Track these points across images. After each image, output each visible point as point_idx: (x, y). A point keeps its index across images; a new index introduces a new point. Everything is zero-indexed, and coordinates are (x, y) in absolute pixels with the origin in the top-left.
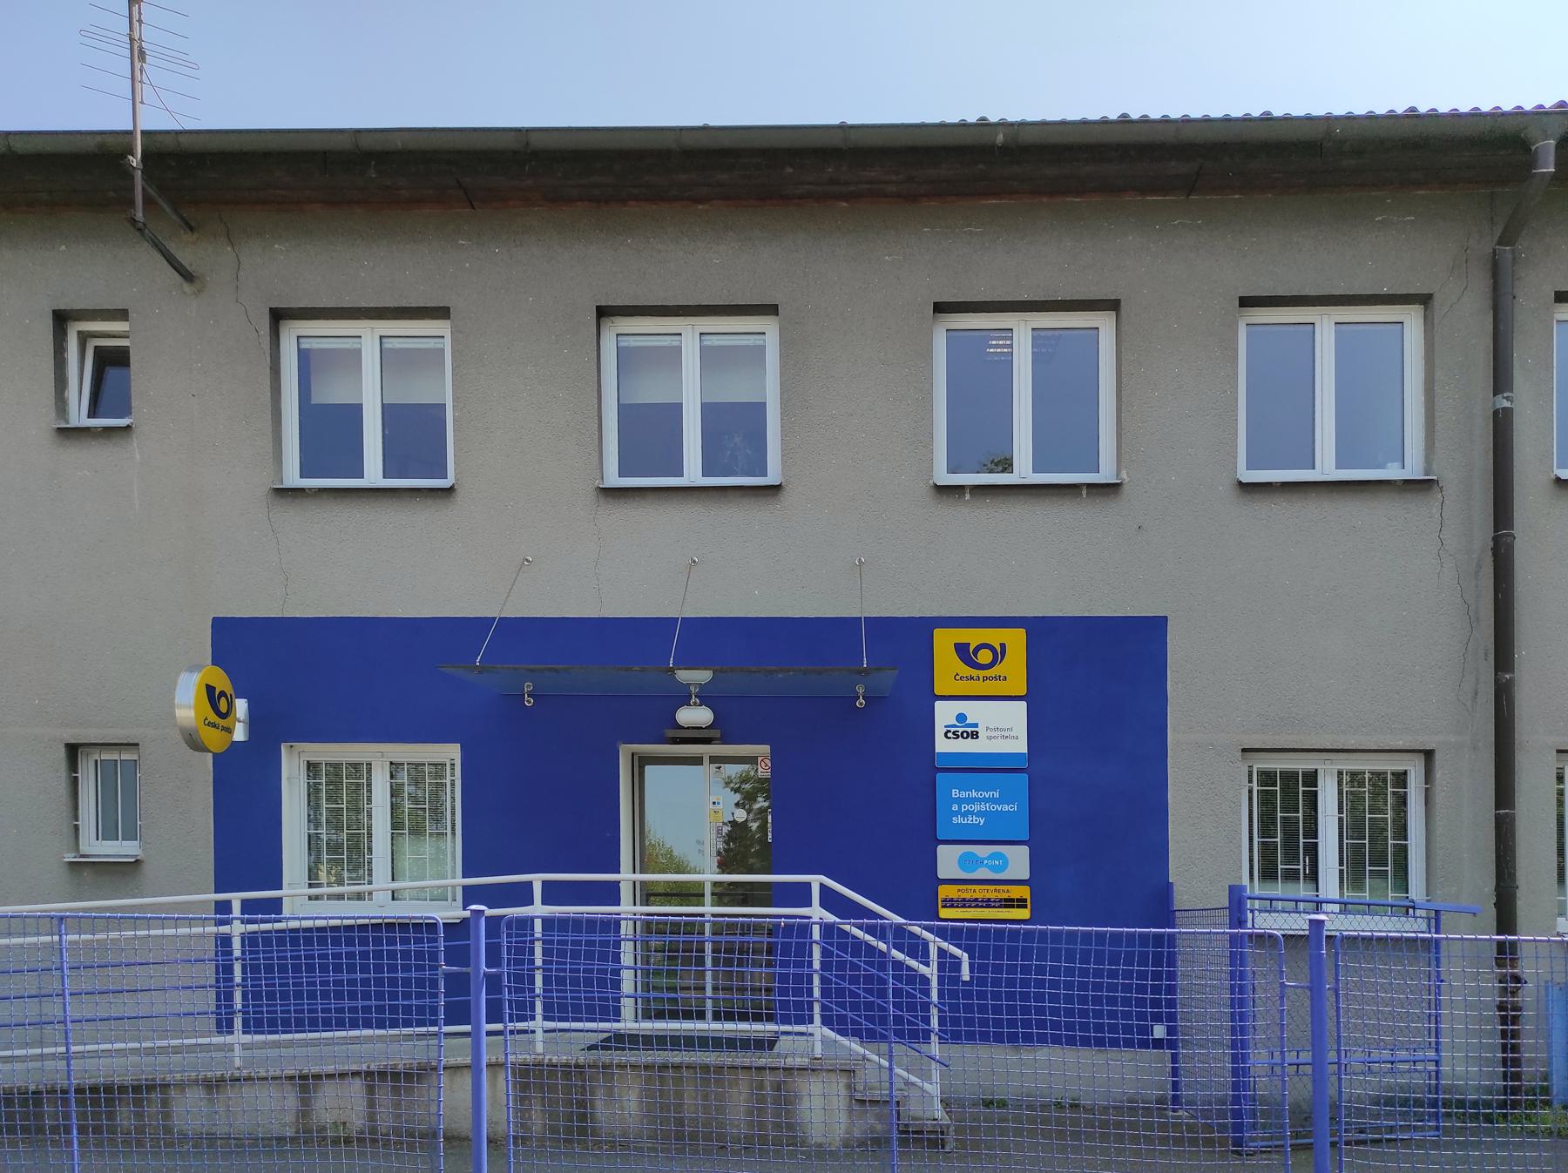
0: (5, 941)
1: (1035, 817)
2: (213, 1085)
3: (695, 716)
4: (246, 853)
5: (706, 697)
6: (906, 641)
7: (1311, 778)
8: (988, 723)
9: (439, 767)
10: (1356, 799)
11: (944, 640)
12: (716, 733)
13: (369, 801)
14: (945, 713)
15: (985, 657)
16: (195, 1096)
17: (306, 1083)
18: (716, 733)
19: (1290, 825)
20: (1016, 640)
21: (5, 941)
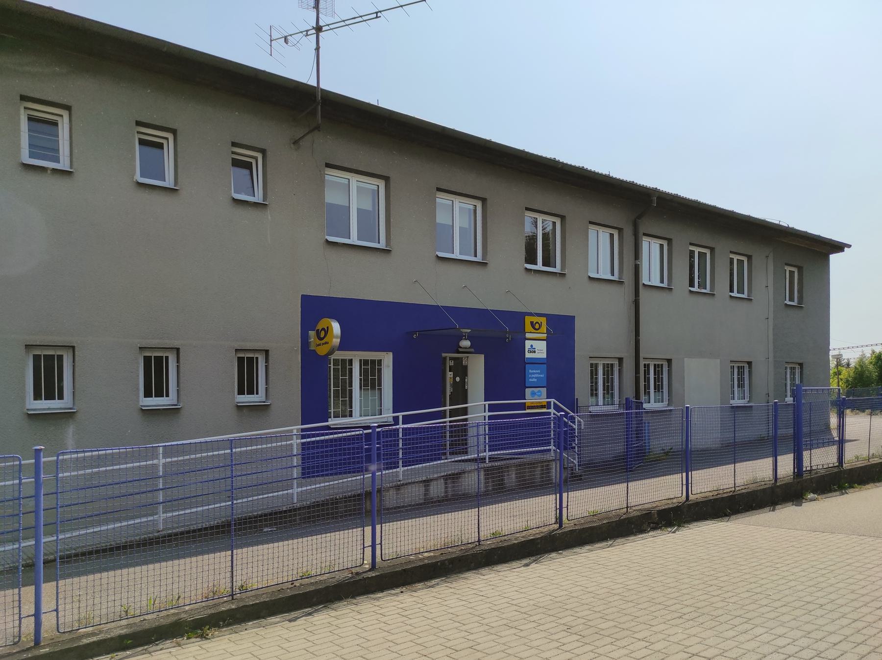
0: (3, 484)
1: (548, 378)
2: (398, 487)
3: (466, 343)
4: (314, 407)
5: (469, 338)
6: (516, 320)
7: (351, 361)
8: (537, 348)
9: (612, 365)
10: (366, 371)
11: (528, 320)
12: (472, 350)
13: (361, 380)
14: (528, 344)
15: (537, 326)
16: (392, 492)
17: (427, 482)
18: (472, 350)
19: (344, 381)
20: (543, 320)
21: (3, 484)
